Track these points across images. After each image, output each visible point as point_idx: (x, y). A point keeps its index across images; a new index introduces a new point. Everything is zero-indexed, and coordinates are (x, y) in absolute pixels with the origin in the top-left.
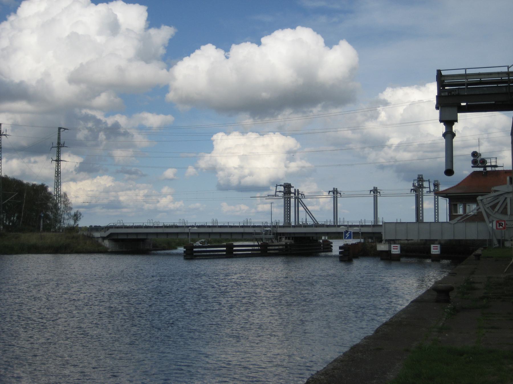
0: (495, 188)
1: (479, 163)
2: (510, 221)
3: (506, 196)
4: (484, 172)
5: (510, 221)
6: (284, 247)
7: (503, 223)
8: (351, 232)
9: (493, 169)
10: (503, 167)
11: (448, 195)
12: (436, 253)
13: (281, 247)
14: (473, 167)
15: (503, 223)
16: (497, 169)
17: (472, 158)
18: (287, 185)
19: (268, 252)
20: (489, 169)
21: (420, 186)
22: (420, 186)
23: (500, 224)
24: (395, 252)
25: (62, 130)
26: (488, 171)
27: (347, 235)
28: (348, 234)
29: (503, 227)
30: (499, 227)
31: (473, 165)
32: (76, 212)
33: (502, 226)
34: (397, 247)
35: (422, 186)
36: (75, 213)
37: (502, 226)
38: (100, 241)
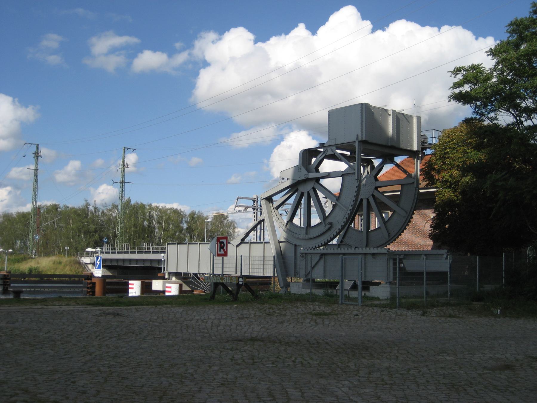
2: (305, 239)
5: (305, 239)
8: (101, 257)
18: (255, 198)
25: (126, 149)
29: (224, 250)
30: (220, 251)
34: (133, 284)
38: (90, 266)
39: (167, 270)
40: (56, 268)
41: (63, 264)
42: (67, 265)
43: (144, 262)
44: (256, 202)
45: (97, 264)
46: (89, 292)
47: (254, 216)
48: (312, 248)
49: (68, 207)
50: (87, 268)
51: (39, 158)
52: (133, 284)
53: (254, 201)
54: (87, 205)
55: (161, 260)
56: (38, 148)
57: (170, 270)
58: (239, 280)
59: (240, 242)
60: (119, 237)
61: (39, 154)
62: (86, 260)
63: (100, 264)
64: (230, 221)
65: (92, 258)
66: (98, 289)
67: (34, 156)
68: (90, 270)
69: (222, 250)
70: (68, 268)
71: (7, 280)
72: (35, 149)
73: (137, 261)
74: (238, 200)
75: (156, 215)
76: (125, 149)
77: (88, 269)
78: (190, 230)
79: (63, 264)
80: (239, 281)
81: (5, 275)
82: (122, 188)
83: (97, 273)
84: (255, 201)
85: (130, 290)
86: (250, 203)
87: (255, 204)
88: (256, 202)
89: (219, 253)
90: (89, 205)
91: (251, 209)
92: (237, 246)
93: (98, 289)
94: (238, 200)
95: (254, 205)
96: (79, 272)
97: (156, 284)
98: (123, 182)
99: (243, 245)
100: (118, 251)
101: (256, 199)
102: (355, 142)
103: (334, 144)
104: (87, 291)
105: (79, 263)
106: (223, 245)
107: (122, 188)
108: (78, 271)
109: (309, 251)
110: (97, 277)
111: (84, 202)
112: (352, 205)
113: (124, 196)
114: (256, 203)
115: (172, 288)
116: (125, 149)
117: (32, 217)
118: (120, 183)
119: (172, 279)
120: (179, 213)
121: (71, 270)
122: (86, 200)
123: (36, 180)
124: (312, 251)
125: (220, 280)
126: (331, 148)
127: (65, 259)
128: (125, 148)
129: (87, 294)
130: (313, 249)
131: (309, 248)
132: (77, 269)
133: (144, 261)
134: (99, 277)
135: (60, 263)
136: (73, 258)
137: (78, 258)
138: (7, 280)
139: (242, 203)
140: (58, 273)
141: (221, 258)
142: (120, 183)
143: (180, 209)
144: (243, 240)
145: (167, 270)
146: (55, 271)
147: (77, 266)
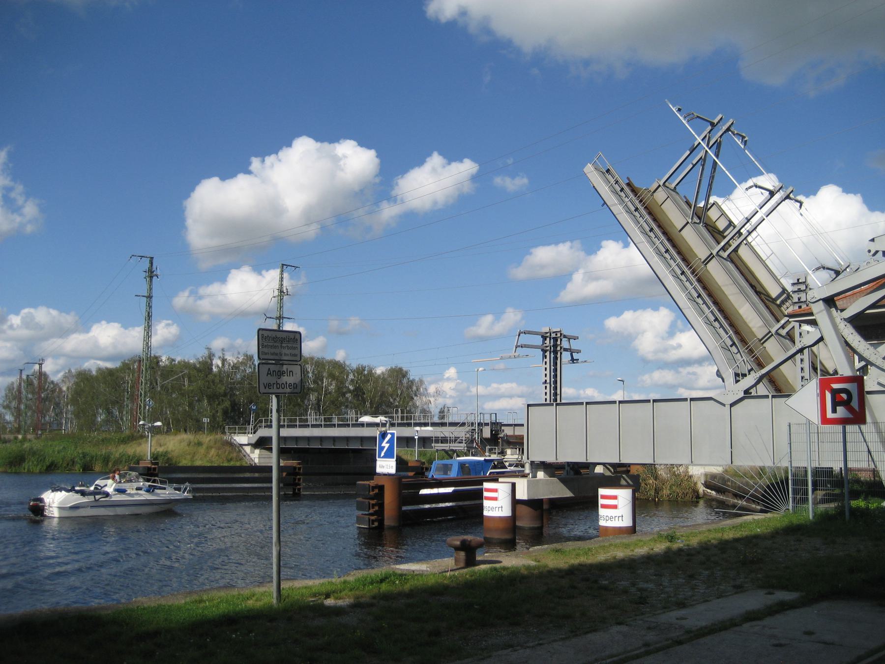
8: (393, 434)
18: (547, 333)
21: (800, 307)
23: (835, 393)
25: (285, 267)
27: (384, 444)
28: (387, 443)
29: (850, 409)
36: (442, 409)
38: (248, 449)
39: (528, 459)
40: (194, 453)
41: (204, 447)
42: (211, 447)
43: (348, 441)
44: (548, 339)
45: (384, 447)
46: (373, 505)
47: (546, 363)
49: (173, 360)
50: (243, 451)
51: (155, 278)
52: (495, 491)
53: (544, 338)
54: (211, 356)
55: (413, 439)
56: (151, 263)
57: (532, 459)
59: (742, 395)
61: (155, 273)
62: (241, 439)
63: (391, 449)
64: (411, 379)
65: (250, 435)
66: (389, 498)
67: (145, 276)
68: (249, 456)
70: (213, 452)
72: (148, 265)
73: (334, 439)
74: (519, 335)
75: (313, 372)
77: (245, 454)
78: (358, 392)
79: (204, 447)
81: (149, 469)
83: (383, 467)
85: (486, 503)
86: (538, 340)
87: (546, 342)
88: (548, 339)
89: (830, 415)
90: (214, 355)
91: (540, 350)
92: (732, 405)
93: (389, 498)
94: (519, 335)
95: (545, 345)
96: (231, 459)
99: (746, 401)
100: (400, 421)
101: (548, 334)
104: (369, 503)
105: (231, 444)
106: (844, 396)
108: (230, 457)
110: (385, 475)
111: (206, 353)
114: (548, 341)
115: (619, 498)
117: (144, 373)
118: (277, 318)
119: (535, 476)
120: (344, 368)
121: (218, 455)
122: (208, 348)
123: (149, 313)
127: (206, 438)
128: (283, 265)
129: (370, 509)
132: (229, 453)
133: (348, 439)
135: (199, 444)
136: (219, 436)
137: (226, 437)
139: (525, 339)
140: (198, 463)
141: (839, 428)
142: (277, 318)
143: (344, 362)
144: (747, 392)
145: (528, 459)
146: (193, 457)
147: (228, 448)
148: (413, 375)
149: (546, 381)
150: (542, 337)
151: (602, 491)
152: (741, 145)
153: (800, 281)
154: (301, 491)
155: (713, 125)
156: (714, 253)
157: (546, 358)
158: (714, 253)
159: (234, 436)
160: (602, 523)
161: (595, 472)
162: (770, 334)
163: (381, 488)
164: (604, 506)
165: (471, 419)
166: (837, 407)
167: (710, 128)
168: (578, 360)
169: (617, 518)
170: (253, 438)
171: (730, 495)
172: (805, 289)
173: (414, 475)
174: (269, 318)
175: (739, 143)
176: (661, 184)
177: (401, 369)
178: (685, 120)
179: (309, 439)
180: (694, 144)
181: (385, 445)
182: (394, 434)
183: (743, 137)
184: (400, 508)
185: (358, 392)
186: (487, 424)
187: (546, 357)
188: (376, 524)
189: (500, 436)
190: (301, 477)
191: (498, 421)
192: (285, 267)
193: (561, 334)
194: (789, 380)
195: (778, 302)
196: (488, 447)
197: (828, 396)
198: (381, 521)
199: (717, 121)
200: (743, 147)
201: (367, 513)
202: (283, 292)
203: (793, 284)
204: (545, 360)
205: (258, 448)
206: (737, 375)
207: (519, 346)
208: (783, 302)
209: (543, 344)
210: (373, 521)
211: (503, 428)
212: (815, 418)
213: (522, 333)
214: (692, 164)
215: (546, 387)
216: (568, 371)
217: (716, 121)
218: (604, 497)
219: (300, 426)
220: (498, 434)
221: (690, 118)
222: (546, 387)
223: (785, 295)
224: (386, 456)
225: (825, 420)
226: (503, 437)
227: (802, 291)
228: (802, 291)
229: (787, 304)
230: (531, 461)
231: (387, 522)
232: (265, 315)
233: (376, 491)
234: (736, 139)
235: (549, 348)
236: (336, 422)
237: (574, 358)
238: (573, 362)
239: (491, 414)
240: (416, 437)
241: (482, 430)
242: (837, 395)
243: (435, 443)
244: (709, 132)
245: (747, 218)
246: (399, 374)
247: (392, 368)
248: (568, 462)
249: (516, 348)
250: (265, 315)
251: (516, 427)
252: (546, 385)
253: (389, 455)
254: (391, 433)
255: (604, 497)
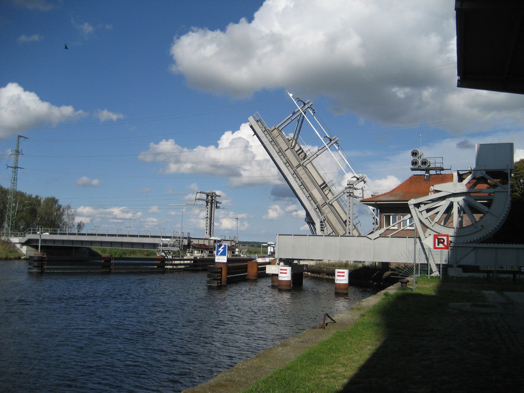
0: (437, 187)
1: (420, 164)
3: (452, 199)
4: (426, 176)
6: (192, 262)
7: (445, 238)
8: (225, 246)
9: (438, 172)
10: (451, 169)
11: (377, 203)
12: (341, 282)
13: (189, 262)
14: (413, 170)
15: (445, 238)
16: (443, 172)
17: (412, 158)
18: (209, 193)
19: (165, 267)
20: (432, 172)
21: (350, 195)
22: (350, 195)
23: (439, 239)
24: (283, 277)
26: (431, 175)
28: (222, 249)
29: (444, 245)
30: (438, 245)
31: (412, 167)
32: (80, 222)
33: (443, 243)
34: (286, 270)
35: (352, 195)
36: (79, 223)
37: (443, 243)
38: (18, 246)
43: (91, 243)
45: (220, 251)
46: (219, 276)
47: (208, 208)
48: (464, 243)
53: (208, 196)
58: (521, 269)
59: (379, 236)
60: (11, 217)
62: (15, 240)
65: (21, 238)
66: (224, 273)
69: (440, 244)
71: (44, 262)
76: (19, 137)
80: (520, 269)
82: (15, 173)
84: (209, 195)
86: (204, 196)
89: (437, 246)
91: (205, 201)
92: (374, 239)
93: (224, 273)
94: (197, 194)
97: (272, 269)
98: (16, 167)
102: (506, 170)
103: (484, 169)
105: (8, 243)
106: (442, 241)
107: (15, 173)
109: (461, 245)
112: (505, 214)
113: (17, 180)
115: (345, 273)
116: (19, 137)
124: (464, 245)
125: (499, 269)
126: (480, 172)
130: (464, 244)
131: (460, 243)
134: (224, 263)
138: (44, 262)
143: (25, 193)
148: (63, 203)
149: (207, 217)
150: (206, 195)
151: (337, 270)
152: (312, 113)
153: (350, 183)
154: (113, 270)
155: (305, 104)
156: (301, 164)
157: (208, 206)
158: (301, 164)
159: (10, 238)
160: (337, 282)
161: (294, 262)
162: (326, 203)
163: (221, 268)
164: (338, 276)
165: (177, 235)
166: (440, 244)
167: (303, 105)
168: (220, 207)
169: (344, 280)
170: (24, 240)
171: (325, 274)
172: (353, 187)
173: (161, 262)
174: (9, 167)
175: (311, 112)
176: (277, 127)
177: (54, 198)
178: (295, 101)
179: (63, 241)
180: (295, 111)
181: (221, 250)
182: (226, 245)
183: (313, 110)
184: (227, 276)
185: (33, 212)
186: (186, 238)
187: (208, 205)
188: (220, 284)
189: (192, 244)
190: (45, 262)
191: (190, 237)
192: (20, 137)
193: (215, 194)
194: (334, 225)
195: (322, 187)
196: (188, 249)
197: (437, 240)
198: (221, 283)
199: (307, 103)
200: (313, 114)
201: (211, 279)
202: (19, 152)
203: (348, 184)
204: (207, 207)
205: (25, 245)
206: (321, 222)
207: (197, 199)
208: (324, 188)
209: (207, 199)
210: (219, 283)
211: (192, 240)
212: (432, 247)
213: (199, 192)
214: (291, 119)
215: (207, 220)
216: (217, 213)
217: (306, 103)
218: (338, 272)
219: (60, 234)
220: (190, 243)
221: (299, 100)
222: (207, 220)
223: (325, 185)
224: (221, 254)
225: (435, 248)
226: (193, 245)
227: (351, 188)
228: (351, 188)
229: (326, 189)
230: (280, 258)
231: (223, 284)
232: (7, 165)
233: (220, 270)
234: (309, 110)
235: (210, 201)
236: (59, 232)
237: (218, 206)
238: (217, 208)
239: (188, 233)
240: (161, 244)
241: (183, 241)
242: (440, 240)
243: (162, 246)
244: (302, 107)
245: (318, 149)
246: (54, 201)
247: (48, 197)
248: (286, 259)
249: (195, 200)
250: (7, 165)
251: (205, 240)
252: (207, 219)
253: (223, 254)
254: (224, 245)
255: (338, 272)
